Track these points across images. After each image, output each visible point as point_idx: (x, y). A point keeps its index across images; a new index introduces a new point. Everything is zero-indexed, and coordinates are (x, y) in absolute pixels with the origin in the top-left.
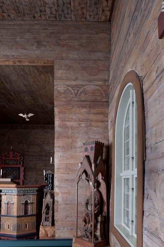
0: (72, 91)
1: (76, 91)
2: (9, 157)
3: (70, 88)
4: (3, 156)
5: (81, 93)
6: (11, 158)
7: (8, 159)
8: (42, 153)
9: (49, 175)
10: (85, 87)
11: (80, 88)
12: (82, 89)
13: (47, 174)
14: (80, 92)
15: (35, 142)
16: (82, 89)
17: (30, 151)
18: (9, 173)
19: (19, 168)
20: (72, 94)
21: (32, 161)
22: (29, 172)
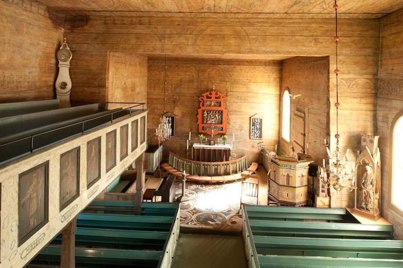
0: (346, 84)
1: (348, 84)
2: (211, 98)
3: (342, 80)
4: (204, 97)
5: (353, 85)
6: (213, 98)
7: (209, 99)
8: (249, 93)
9: (256, 120)
10: (356, 80)
11: (353, 81)
12: (354, 82)
13: (255, 119)
14: (352, 84)
15: (240, 80)
16: (354, 82)
17: (234, 91)
18: (210, 116)
19: (222, 112)
20: (345, 86)
21: (236, 102)
22: (233, 116)
